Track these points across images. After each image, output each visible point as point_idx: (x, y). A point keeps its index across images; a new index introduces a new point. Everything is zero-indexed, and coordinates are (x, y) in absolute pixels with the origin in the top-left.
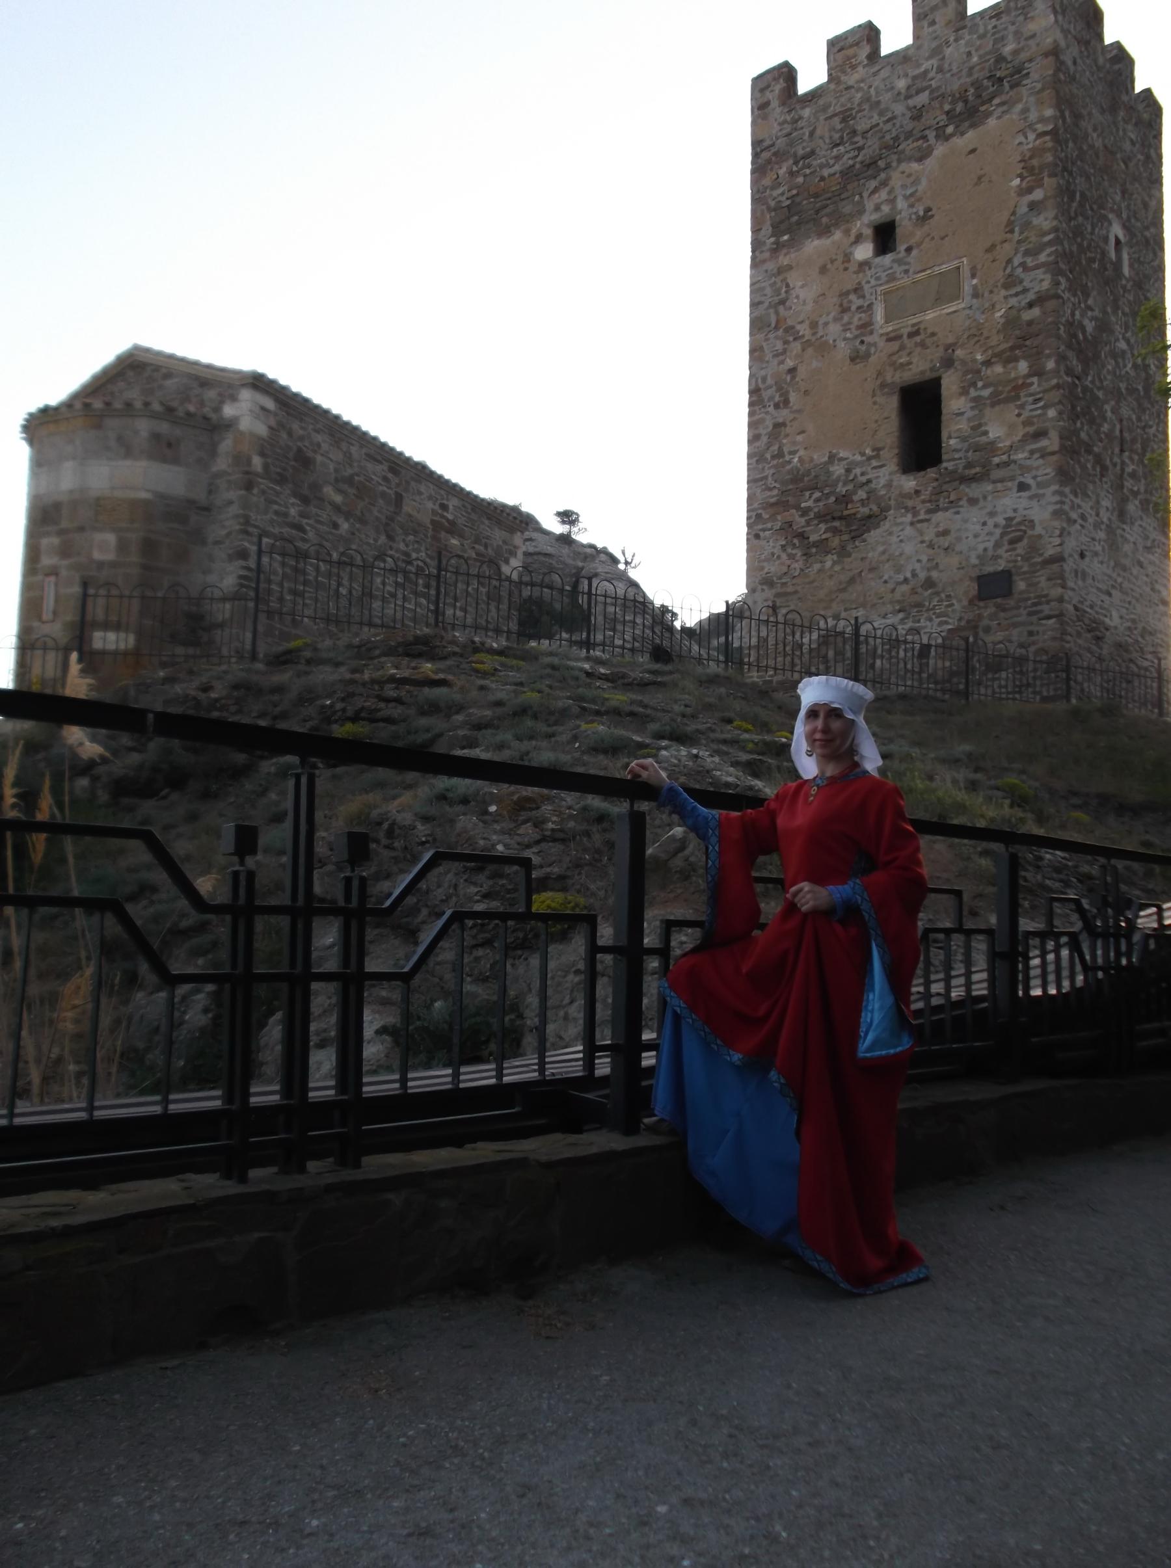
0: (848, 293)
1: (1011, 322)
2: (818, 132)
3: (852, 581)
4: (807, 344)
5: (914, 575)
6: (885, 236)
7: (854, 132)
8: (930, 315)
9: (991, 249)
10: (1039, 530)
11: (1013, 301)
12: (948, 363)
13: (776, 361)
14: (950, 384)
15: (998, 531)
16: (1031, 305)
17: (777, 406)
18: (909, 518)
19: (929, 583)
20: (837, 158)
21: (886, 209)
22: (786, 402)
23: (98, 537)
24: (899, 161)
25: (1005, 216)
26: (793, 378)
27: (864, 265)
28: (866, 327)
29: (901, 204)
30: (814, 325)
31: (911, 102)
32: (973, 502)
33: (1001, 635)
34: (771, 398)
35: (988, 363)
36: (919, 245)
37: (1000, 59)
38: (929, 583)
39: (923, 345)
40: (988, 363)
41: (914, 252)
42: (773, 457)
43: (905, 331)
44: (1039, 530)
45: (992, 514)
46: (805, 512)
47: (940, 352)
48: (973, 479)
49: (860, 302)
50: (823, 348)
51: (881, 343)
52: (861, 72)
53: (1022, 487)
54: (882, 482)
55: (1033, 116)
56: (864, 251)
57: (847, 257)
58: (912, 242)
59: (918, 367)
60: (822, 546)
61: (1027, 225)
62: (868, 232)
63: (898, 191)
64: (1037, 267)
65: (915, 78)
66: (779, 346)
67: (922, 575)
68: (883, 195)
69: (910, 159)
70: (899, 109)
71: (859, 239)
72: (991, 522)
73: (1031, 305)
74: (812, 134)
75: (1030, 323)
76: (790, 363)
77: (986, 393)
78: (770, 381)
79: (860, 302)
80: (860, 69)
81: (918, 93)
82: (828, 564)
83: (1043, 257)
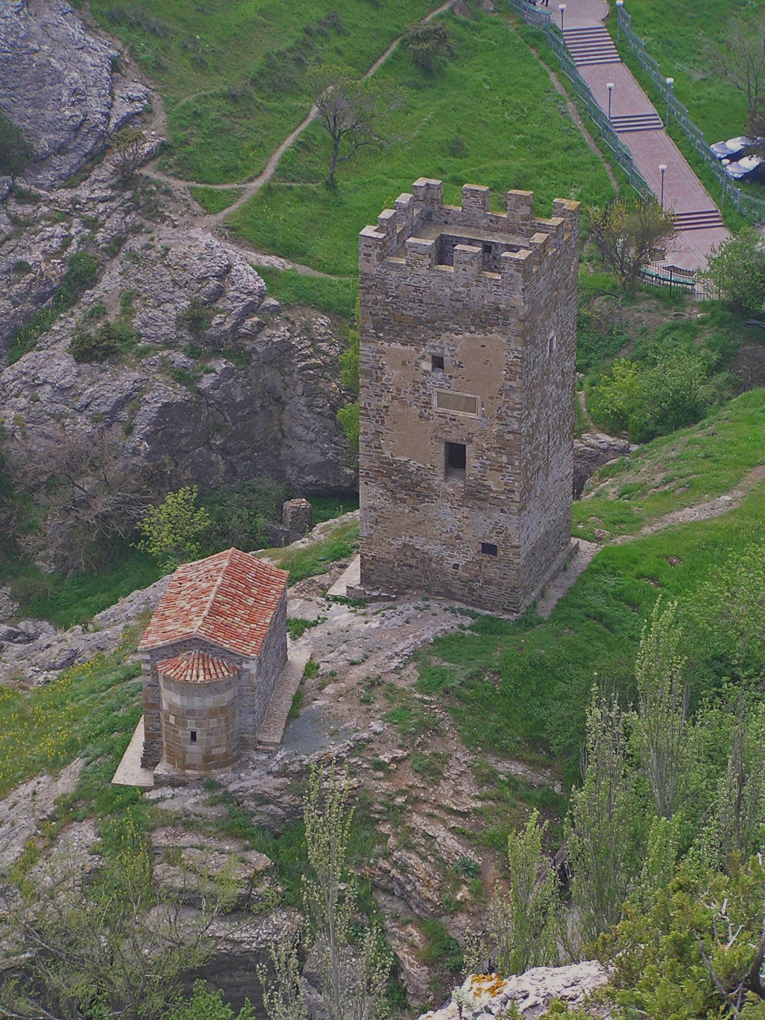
0: (418, 383)
1: (499, 436)
2: (400, 288)
3: (419, 523)
4: (394, 398)
5: (451, 531)
6: (438, 363)
7: (421, 301)
8: (461, 414)
9: (492, 398)
10: (509, 532)
11: (501, 427)
12: (470, 441)
13: (377, 398)
14: (470, 450)
15: (491, 526)
16: (509, 432)
17: (377, 421)
18: (449, 504)
19: (458, 537)
20: (412, 309)
21: (439, 351)
22: (383, 422)
23: (211, 720)
24: (447, 330)
25: (498, 386)
26: (387, 411)
27: (426, 372)
28: (427, 404)
29: (446, 352)
30: (398, 390)
31: (453, 303)
32: (480, 509)
33: (492, 571)
34: (375, 417)
35: (488, 450)
36: (456, 378)
37: (498, 309)
38: (458, 537)
39: (457, 426)
40: (488, 450)
41: (453, 380)
42: (375, 447)
43: (449, 417)
44: (509, 532)
45: (489, 518)
46: (394, 482)
47: (465, 436)
48: (480, 499)
49: (424, 390)
50: (404, 404)
51: (436, 416)
52: (424, 271)
53: (502, 511)
54: (436, 483)
55: (513, 346)
56: (427, 366)
57: (417, 364)
58: (453, 374)
59: (455, 436)
60: (404, 501)
61: (508, 396)
62: (430, 357)
63: (445, 345)
64: (512, 417)
65: (454, 292)
66: (378, 391)
67: (456, 533)
68: (437, 343)
69: (451, 330)
70: (446, 303)
71: (423, 357)
72: (488, 521)
73: (509, 432)
74: (397, 287)
75: (508, 440)
76: (384, 403)
77: (488, 463)
78: (372, 407)
79: (424, 390)
80: (425, 268)
81: (457, 300)
82: (407, 511)
83: (515, 413)
